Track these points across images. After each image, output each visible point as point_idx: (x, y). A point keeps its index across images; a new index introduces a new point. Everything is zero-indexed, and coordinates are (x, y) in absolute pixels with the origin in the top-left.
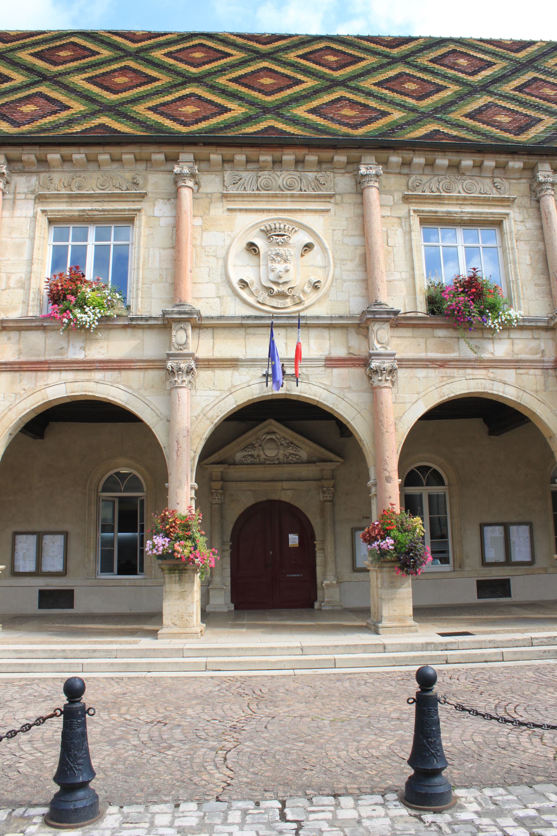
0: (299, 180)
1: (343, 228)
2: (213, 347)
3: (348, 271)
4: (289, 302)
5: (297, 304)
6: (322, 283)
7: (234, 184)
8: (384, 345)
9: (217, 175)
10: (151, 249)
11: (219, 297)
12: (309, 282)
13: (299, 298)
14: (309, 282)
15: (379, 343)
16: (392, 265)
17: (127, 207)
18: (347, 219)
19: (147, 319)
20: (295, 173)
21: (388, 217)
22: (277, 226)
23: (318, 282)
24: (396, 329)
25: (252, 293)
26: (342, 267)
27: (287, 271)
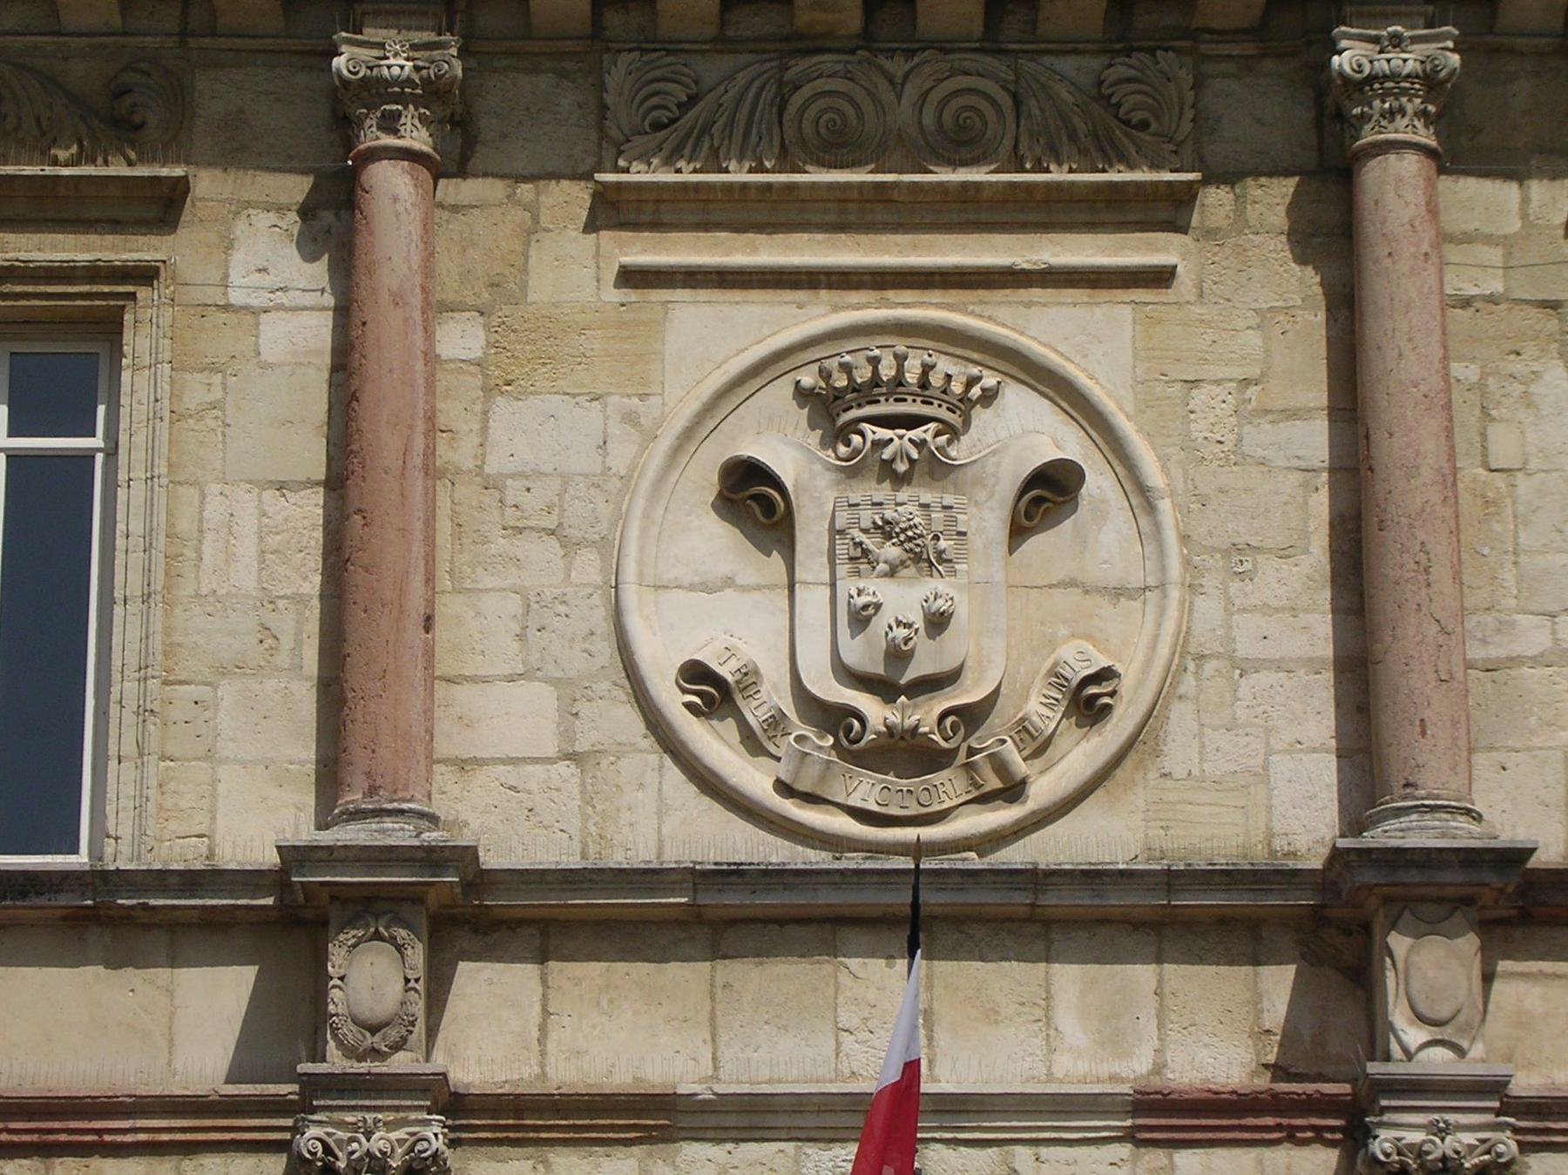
0: (1006, 101)
1: (1239, 373)
2: (543, 1028)
3: (1266, 609)
4: (948, 786)
5: (984, 799)
6: (1126, 685)
7: (658, 126)
8: (1446, 1033)
9: (563, 75)
10: (213, 488)
11: (572, 757)
12: (1056, 676)
13: (1000, 766)
14: (1056, 676)
15: (1422, 1019)
16: (1509, 576)
17: (83, 257)
18: (1264, 318)
19: (192, 881)
20: (988, 61)
21: (1492, 300)
22: (887, 371)
23: (1105, 675)
24: (1518, 933)
25: (752, 743)
26: (1235, 586)
27: (938, 622)
